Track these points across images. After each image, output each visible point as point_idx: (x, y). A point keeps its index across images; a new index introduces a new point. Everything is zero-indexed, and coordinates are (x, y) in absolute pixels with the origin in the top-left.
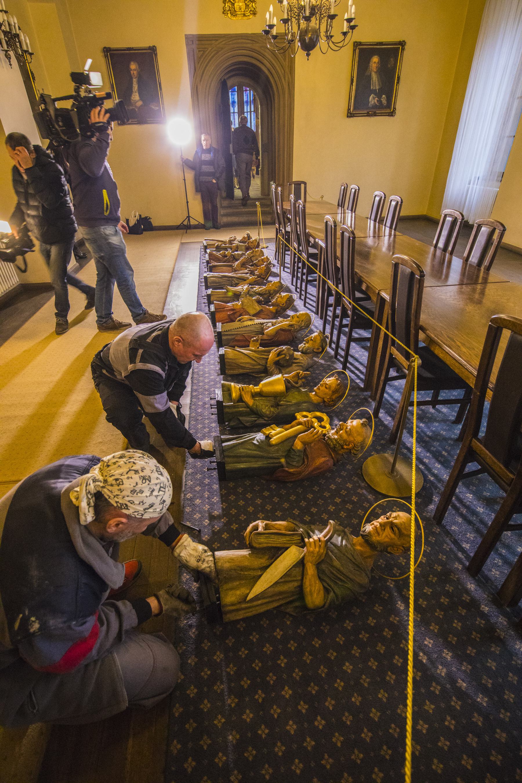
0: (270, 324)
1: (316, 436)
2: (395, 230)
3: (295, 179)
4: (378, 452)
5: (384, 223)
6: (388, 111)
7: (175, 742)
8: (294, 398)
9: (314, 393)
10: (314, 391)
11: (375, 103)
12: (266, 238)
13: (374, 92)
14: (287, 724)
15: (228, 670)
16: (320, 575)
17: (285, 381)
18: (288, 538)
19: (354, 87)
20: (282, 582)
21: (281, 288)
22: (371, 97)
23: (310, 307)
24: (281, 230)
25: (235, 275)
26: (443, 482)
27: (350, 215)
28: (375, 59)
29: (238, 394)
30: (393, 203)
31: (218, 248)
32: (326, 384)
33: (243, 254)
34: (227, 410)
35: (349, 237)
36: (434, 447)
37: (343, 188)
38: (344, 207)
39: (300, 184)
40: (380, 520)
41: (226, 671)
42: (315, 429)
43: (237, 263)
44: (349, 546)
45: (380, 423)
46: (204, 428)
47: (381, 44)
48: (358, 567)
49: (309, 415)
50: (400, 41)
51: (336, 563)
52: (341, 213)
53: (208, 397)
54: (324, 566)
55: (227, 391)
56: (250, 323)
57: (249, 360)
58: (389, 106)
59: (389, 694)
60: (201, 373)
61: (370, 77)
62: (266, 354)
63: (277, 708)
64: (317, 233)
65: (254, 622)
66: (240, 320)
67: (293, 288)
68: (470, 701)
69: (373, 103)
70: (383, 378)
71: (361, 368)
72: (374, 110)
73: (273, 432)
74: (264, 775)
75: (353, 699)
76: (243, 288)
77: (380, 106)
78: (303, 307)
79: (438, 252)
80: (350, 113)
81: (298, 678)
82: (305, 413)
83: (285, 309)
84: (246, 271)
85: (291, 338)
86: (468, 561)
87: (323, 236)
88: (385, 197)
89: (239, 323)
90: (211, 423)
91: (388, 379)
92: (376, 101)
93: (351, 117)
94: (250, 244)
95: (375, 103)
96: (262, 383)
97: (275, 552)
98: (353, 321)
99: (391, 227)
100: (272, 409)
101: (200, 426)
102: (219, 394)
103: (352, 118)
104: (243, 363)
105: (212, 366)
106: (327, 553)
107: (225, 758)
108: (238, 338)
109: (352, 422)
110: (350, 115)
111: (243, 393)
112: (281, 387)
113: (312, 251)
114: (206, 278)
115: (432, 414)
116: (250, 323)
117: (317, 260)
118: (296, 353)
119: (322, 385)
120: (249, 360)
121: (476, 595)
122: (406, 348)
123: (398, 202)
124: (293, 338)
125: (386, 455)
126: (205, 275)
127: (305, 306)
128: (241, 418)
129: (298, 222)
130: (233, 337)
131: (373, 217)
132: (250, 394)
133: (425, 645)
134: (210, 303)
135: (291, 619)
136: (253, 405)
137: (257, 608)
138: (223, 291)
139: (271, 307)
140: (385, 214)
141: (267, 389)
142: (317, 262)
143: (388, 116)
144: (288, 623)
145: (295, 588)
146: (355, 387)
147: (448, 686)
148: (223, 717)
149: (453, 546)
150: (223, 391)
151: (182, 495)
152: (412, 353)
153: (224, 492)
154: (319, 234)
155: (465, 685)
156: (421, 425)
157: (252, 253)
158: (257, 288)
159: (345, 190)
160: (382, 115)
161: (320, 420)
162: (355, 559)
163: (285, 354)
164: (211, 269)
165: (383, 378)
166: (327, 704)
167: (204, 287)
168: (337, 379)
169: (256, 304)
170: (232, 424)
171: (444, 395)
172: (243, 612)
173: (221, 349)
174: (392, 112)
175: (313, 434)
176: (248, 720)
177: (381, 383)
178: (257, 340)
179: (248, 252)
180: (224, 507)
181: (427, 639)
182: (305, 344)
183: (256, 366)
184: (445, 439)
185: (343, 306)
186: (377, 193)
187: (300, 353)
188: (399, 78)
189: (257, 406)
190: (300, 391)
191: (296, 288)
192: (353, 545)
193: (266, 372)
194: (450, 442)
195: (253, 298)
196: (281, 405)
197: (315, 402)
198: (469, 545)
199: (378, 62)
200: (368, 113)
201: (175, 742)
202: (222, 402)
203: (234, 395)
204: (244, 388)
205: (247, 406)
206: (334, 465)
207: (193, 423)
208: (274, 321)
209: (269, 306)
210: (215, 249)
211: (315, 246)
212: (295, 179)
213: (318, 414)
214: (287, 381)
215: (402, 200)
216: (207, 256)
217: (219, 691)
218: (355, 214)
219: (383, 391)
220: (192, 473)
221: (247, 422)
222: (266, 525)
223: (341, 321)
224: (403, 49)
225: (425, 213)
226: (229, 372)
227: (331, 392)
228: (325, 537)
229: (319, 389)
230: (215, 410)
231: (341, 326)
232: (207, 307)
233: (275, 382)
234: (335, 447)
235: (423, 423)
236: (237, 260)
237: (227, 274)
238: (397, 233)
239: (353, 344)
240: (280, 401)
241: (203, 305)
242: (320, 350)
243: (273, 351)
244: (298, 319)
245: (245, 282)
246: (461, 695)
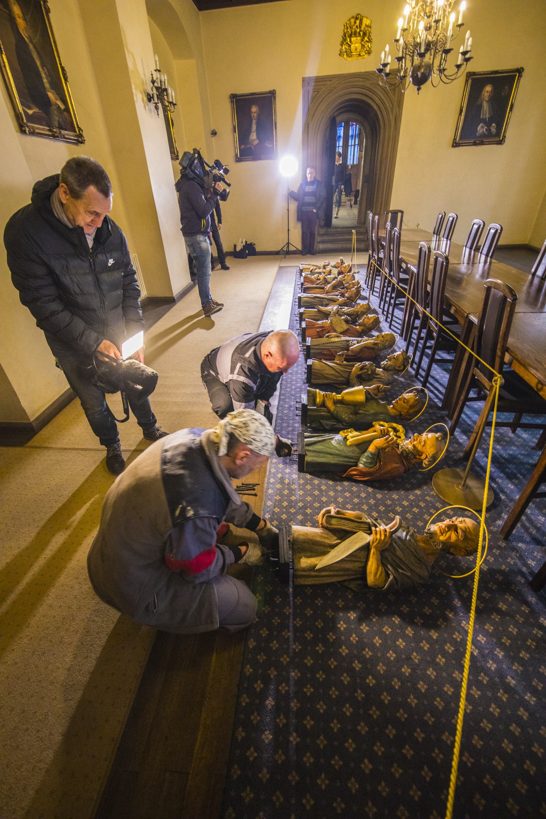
0: (355, 342)
1: (391, 442)
2: (491, 257)
3: (392, 207)
4: (449, 466)
5: (480, 251)
6: (497, 139)
7: (248, 666)
8: (372, 408)
9: (392, 406)
10: (393, 404)
11: (483, 132)
12: (357, 263)
13: (484, 121)
14: (342, 675)
15: (295, 622)
16: (384, 562)
17: (365, 392)
18: (357, 524)
19: (462, 117)
20: (348, 560)
21: (369, 310)
22: (480, 125)
23: (395, 329)
24: (374, 257)
25: (326, 297)
26: (514, 501)
27: (445, 242)
28: (488, 88)
29: (322, 399)
30: (492, 231)
31: (312, 272)
32: (405, 399)
33: (336, 278)
34: (310, 413)
35: (443, 262)
36: (509, 469)
37: (440, 216)
38: (439, 235)
39: (397, 213)
40: (445, 522)
41: (294, 624)
42: (390, 436)
43: (329, 286)
44: (412, 541)
45: (454, 440)
46: (288, 426)
48: (419, 560)
49: (386, 424)
50: (518, 69)
51: (399, 553)
52: (436, 241)
53: (293, 401)
54: (387, 554)
55: (312, 397)
56: (336, 339)
57: (333, 372)
58: (498, 134)
59: (437, 673)
60: (289, 380)
61: (481, 106)
62: (349, 368)
63: (334, 661)
64: (410, 259)
65: (319, 589)
66: (328, 337)
67: (380, 311)
68: (517, 697)
69: (481, 131)
70: (462, 397)
71: (441, 389)
73: (350, 435)
74: (319, 709)
75: (403, 670)
76: (333, 308)
77: (489, 135)
78: (388, 329)
79: (536, 281)
81: (354, 641)
82: (382, 423)
83: (370, 329)
84: (337, 293)
85: (375, 355)
86: (531, 576)
87: (416, 262)
88: (484, 226)
89: (327, 338)
90: (295, 423)
91: (467, 399)
93: (455, 147)
94: (343, 269)
95: (483, 132)
96: (344, 392)
97: (344, 535)
98: (437, 343)
99: (487, 255)
100: (351, 416)
101: (285, 425)
102: (304, 399)
103: (457, 148)
104: (328, 374)
105: (299, 376)
106: (391, 544)
107: (287, 688)
108: (325, 352)
109: (427, 435)
110: (455, 145)
111: (326, 399)
112: (361, 398)
113: (402, 276)
114: (300, 298)
115: (510, 438)
116: (336, 339)
117: (407, 285)
118: (378, 369)
119: (400, 399)
120: (333, 372)
121: (536, 608)
122: (490, 368)
123: (497, 230)
124: (376, 356)
125: (458, 470)
126: (299, 295)
127: (390, 328)
128: (322, 421)
129: (392, 248)
130: (320, 351)
131: (469, 245)
132: (332, 400)
133: (478, 640)
134: (301, 319)
135: (352, 594)
136: (335, 410)
137: (324, 579)
138: (315, 310)
139: (358, 327)
140: (481, 243)
141: (348, 398)
142: (406, 287)
143: (497, 144)
144: (350, 597)
145: (359, 568)
146: (432, 405)
147: (496, 679)
148: (288, 657)
149: (517, 561)
150: (308, 396)
151: (266, 479)
152: (495, 372)
153: (302, 481)
154: (412, 260)
155: (514, 682)
156: (498, 447)
157: (344, 277)
158: (346, 309)
159: (443, 219)
160: (490, 143)
161: (396, 430)
162: (417, 553)
163: (368, 369)
164: (305, 290)
165: (462, 397)
166: (378, 668)
167: (297, 306)
168: (416, 395)
169: (344, 323)
170: (314, 425)
171: (526, 419)
172: (312, 579)
173: (308, 360)
174: (502, 141)
175: (388, 440)
176: (309, 664)
177: (460, 403)
178: (342, 355)
179: (340, 276)
180: (301, 494)
181: (480, 636)
182: (387, 361)
183: (339, 377)
184: (523, 464)
185: (429, 328)
186: (476, 221)
187: (381, 370)
188: (512, 106)
189: (337, 412)
190: (378, 403)
191: (383, 310)
192: (416, 541)
193: (349, 384)
194: (527, 466)
195: (342, 318)
196: (359, 414)
197: (392, 414)
198: (535, 563)
199: (491, 91)
200: (475, 142)
201: (248, 666)
202: (306, 406)
203: (318, 400)
204: (328, 395)
205: (329, 411)
206: (404, 472)
207: (279, 421)
208: (360, 339)
209: (356, 326)
210: (309, 273)
211: (407, 271)
212: (392, 207)
213: (395, 425)
214: (367, 393)
215: (502, 228)
216: (302, 278)
217: (286, 637)
218: (450, 242)
219: (461, 411)
220: (276, 462)
221: (327, 425)
222: (337, 511)
223: (425, 343)
224: (520, 76)
225: (527, 243)
226: (313, 381)
227: (408, 407)
228: (391, 529)
229: (397, 402)
230: (299, 413)
231: (425, 347)
232: (299, 324)
233: (356, 393)
234: (407, 456)
235: (500, 445)
236: (329, 283)
237: (319, 295)
238: (493, 261)
239: (434, 366)
240: (359, 410)
241: (295, 322)
242: (402, 368)
243: (357, 365)
244: (382, 339)
245: (335, 303)
246: (508, 689)
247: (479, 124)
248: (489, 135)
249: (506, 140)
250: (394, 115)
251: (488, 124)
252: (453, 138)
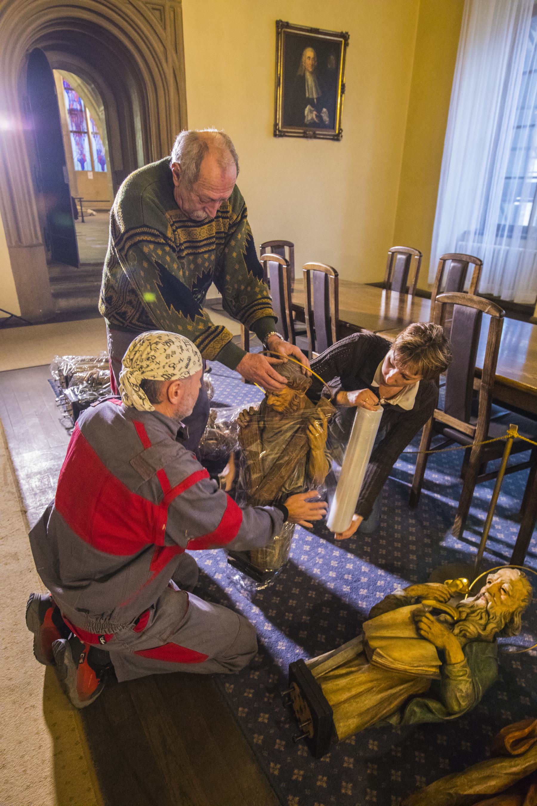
6: (331, 133)
11: (312, 119)
13: (310, 101)
28: (309, 53)
47: (316, 31)
50: (342, 33)
61: (303, 79)
72: (314, 129)
77: (319, 124)
80: (279, 131)
95: (312, 119)
103: (281, 139)
110: (278, 134)
143: (333, 139)
160: (325, 138)
188: (343, 86)
199: (314, 58)
200: (304, 133)
224: (346, 45)
247: (306, 107)
248: (319, 124)
249: (343, 134)
251: (318, 108)
252: (272, 122)
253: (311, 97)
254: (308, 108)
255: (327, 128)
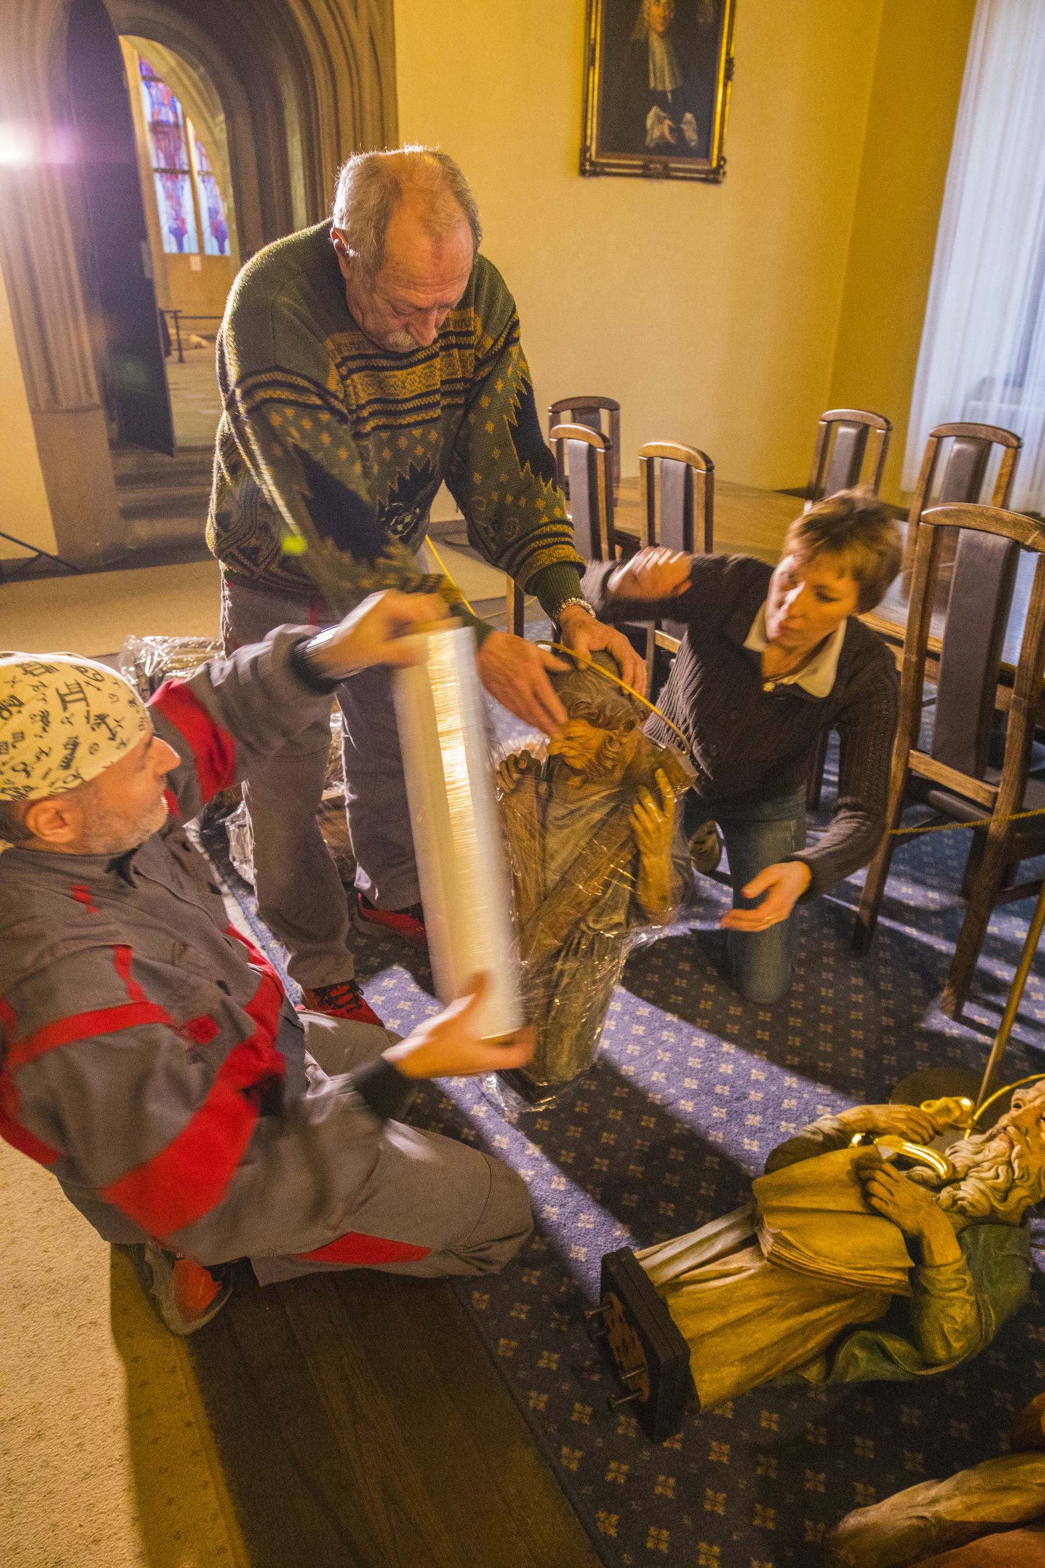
11: (662, 136)
13: (658, 98)
19: (595, 78)
61: (643, 50)
69: (656, 134)
72: (664, 158)
77: (677, 148)
80: (592, 164)
92: (666, 131)
93: (595, 174)
95: (662, 136)
103: (594, 181)
110: (589, 169)
188: (730, 62)
200: (644, 167)
247: (648, 111)
248: (677, 148)
249: (727, 168)
250: (364, 21)
253: (660, 88)
254: (654, 111)
255: (693, 157)
